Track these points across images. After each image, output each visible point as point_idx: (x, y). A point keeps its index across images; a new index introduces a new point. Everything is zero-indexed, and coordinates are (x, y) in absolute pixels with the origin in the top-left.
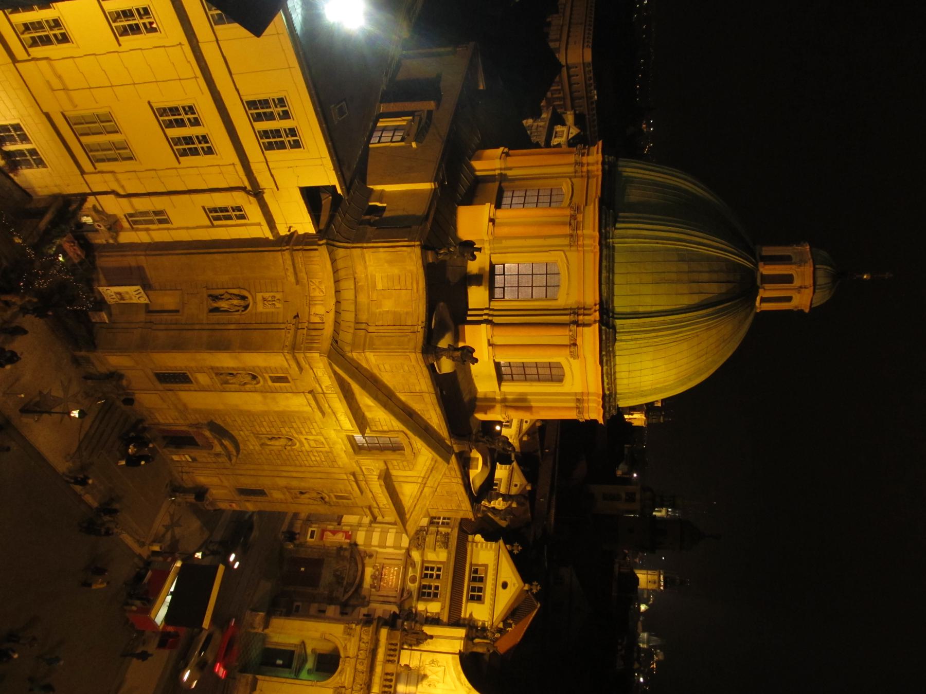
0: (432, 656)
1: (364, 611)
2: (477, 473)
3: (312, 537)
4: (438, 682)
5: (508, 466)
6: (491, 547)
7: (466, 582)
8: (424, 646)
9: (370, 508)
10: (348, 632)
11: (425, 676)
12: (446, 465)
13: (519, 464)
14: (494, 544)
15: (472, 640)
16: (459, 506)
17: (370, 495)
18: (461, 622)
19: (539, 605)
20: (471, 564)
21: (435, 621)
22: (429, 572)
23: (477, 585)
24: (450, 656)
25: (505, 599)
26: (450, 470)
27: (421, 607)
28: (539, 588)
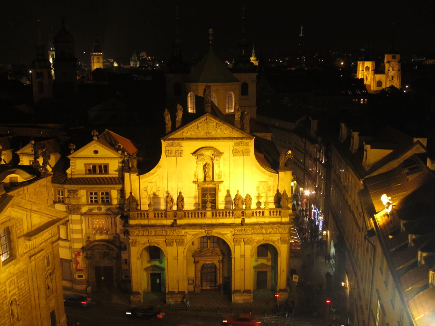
0: (142, 191)
1: (122, 236)
2: (20, 177)
3: (82, 276)
4: (156, 186)
5: (20, 157)
6: (73, 163)
7: (96, 176)
9: (53, 243)
10: (135, 243)
11: (154, 194)
12: (14, 198)
13: (18, 149)
14: (72, 161)
15: (130, 168)
16: (44, 186)
17: (44, 244)
18: (121, 176)
19: (107, 130)
20: (86, 174)
21: (122, 192)
22: (94, 200)
23: (98, 169)
24: (141, 181)
25: (104, 151)
26: (18, 195)
27: (115, 202)
28: (95, 131)
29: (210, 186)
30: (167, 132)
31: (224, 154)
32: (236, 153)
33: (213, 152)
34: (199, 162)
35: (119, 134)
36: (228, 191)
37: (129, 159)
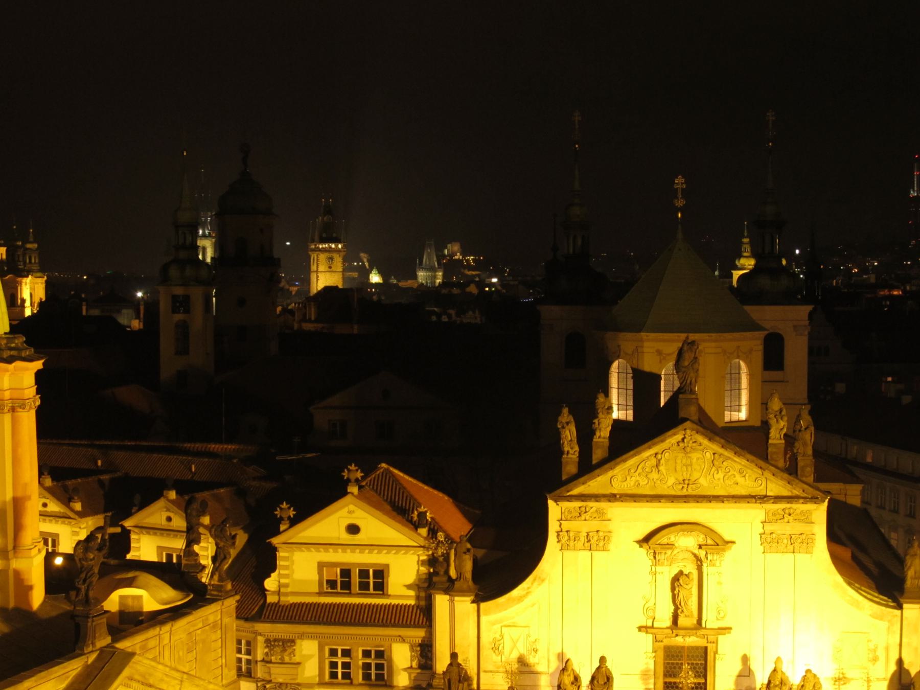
2: (150, 596)
4: (528, 636)
5: (133, 536)
6: (286, 559)
7: (353, 598)
8: (472, 670)
11: (522, 661)
12: (136, 658)
13: (128, 515)
14: (281, 554)
15: (451, 581)
16: (214, 626)
18: (423, 603)
19: (384, 465)
20: (320, 593)
21: (426, 651)
22: (340, 670)
23: (355, 579)
25: (378, 528)
26: (145, 649)
28: (353, 467)
29: (692, 640)
30: (564, 477)
31: (734, 546)
32: (769, 541)
33: (701, 539)
34: (659, 569)
35: (424, 482)
36: (745, 659)
37: (448, 554)
